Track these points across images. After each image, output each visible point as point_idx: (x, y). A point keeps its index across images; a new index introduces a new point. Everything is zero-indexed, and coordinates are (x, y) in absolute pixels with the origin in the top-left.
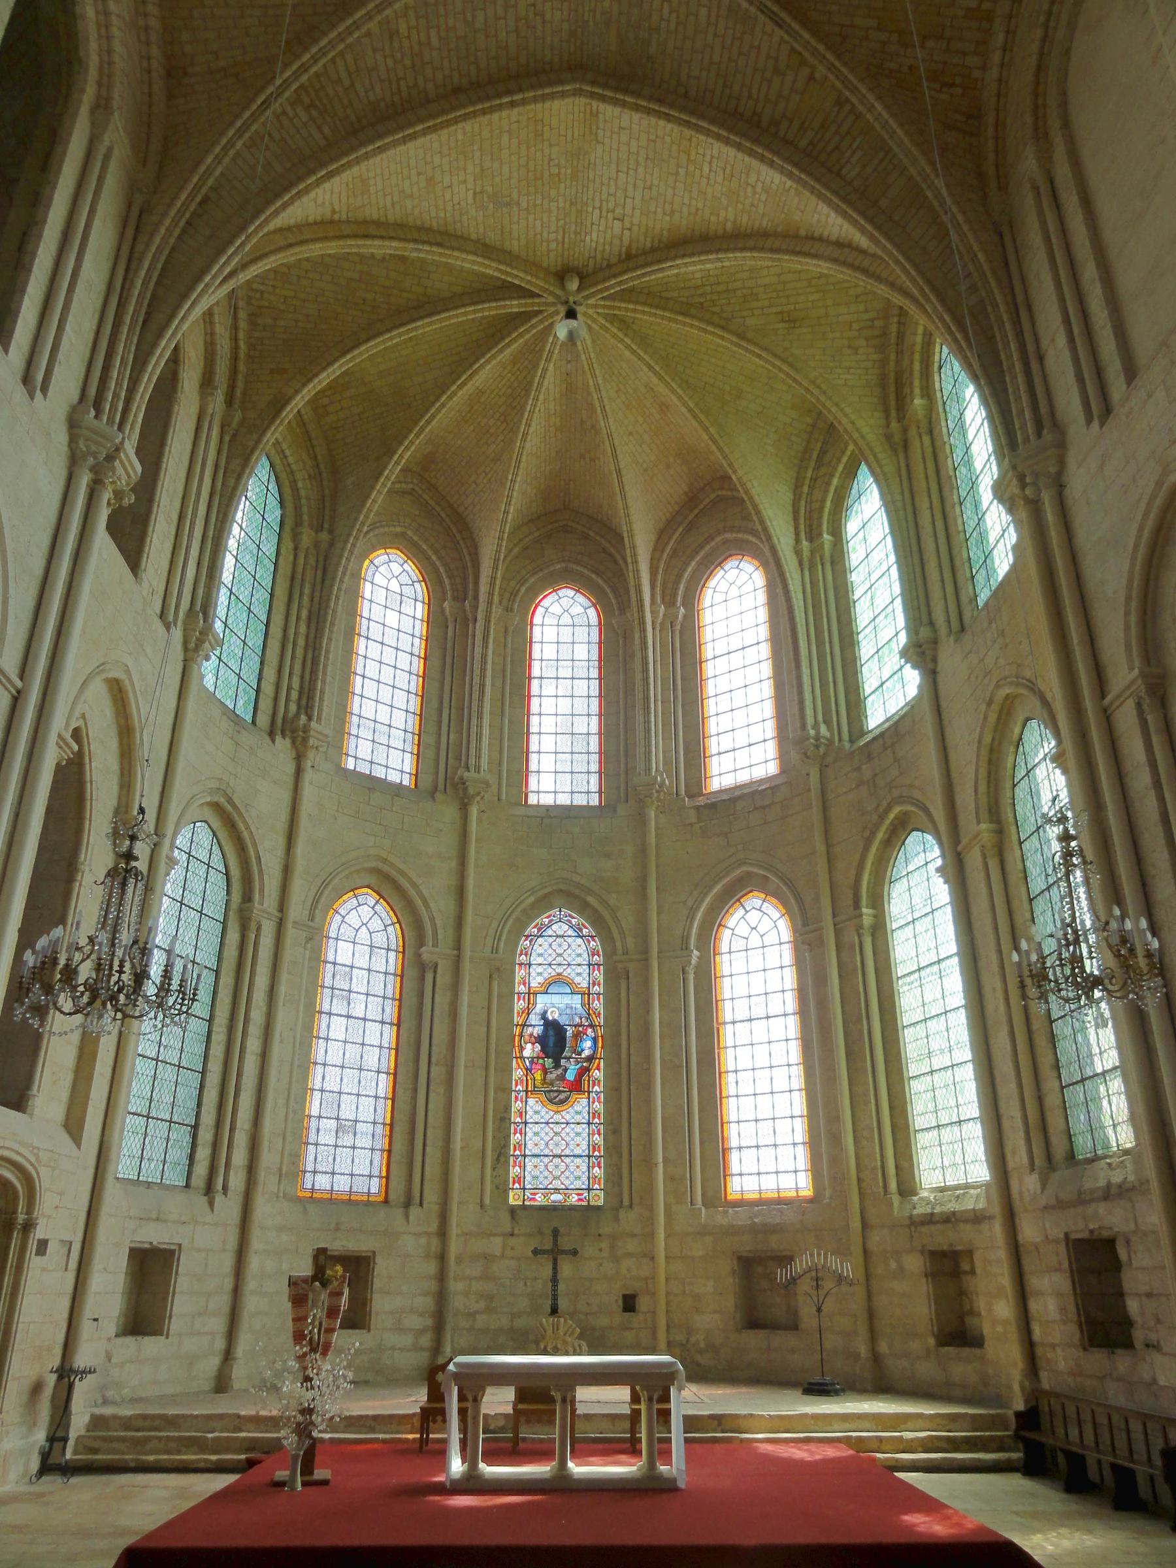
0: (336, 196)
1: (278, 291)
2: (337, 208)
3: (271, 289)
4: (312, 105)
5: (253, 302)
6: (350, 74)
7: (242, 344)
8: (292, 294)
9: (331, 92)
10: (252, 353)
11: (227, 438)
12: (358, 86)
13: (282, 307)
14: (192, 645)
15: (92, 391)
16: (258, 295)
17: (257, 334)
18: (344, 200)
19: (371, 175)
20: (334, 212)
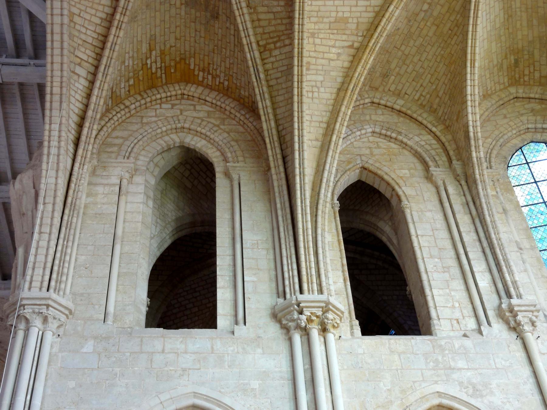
0: (338, 44)
1: (424, 84)
2: (350, 43)
3: (422, 89)
4: (274, 43)
5: (424, 103)
6: (269, 12)
7: (434, 129)
8: (429, 76)
9: (272, 28)
10: (447, 124)
11: (463, 183)
12: (275, 10)
13: (434, 87)
14: (512, 323)
15: (281, 289)
16: (422, 98)
17: (440, 114)
18: (344, 37)
19: (334, 14)
20: (351, 47)
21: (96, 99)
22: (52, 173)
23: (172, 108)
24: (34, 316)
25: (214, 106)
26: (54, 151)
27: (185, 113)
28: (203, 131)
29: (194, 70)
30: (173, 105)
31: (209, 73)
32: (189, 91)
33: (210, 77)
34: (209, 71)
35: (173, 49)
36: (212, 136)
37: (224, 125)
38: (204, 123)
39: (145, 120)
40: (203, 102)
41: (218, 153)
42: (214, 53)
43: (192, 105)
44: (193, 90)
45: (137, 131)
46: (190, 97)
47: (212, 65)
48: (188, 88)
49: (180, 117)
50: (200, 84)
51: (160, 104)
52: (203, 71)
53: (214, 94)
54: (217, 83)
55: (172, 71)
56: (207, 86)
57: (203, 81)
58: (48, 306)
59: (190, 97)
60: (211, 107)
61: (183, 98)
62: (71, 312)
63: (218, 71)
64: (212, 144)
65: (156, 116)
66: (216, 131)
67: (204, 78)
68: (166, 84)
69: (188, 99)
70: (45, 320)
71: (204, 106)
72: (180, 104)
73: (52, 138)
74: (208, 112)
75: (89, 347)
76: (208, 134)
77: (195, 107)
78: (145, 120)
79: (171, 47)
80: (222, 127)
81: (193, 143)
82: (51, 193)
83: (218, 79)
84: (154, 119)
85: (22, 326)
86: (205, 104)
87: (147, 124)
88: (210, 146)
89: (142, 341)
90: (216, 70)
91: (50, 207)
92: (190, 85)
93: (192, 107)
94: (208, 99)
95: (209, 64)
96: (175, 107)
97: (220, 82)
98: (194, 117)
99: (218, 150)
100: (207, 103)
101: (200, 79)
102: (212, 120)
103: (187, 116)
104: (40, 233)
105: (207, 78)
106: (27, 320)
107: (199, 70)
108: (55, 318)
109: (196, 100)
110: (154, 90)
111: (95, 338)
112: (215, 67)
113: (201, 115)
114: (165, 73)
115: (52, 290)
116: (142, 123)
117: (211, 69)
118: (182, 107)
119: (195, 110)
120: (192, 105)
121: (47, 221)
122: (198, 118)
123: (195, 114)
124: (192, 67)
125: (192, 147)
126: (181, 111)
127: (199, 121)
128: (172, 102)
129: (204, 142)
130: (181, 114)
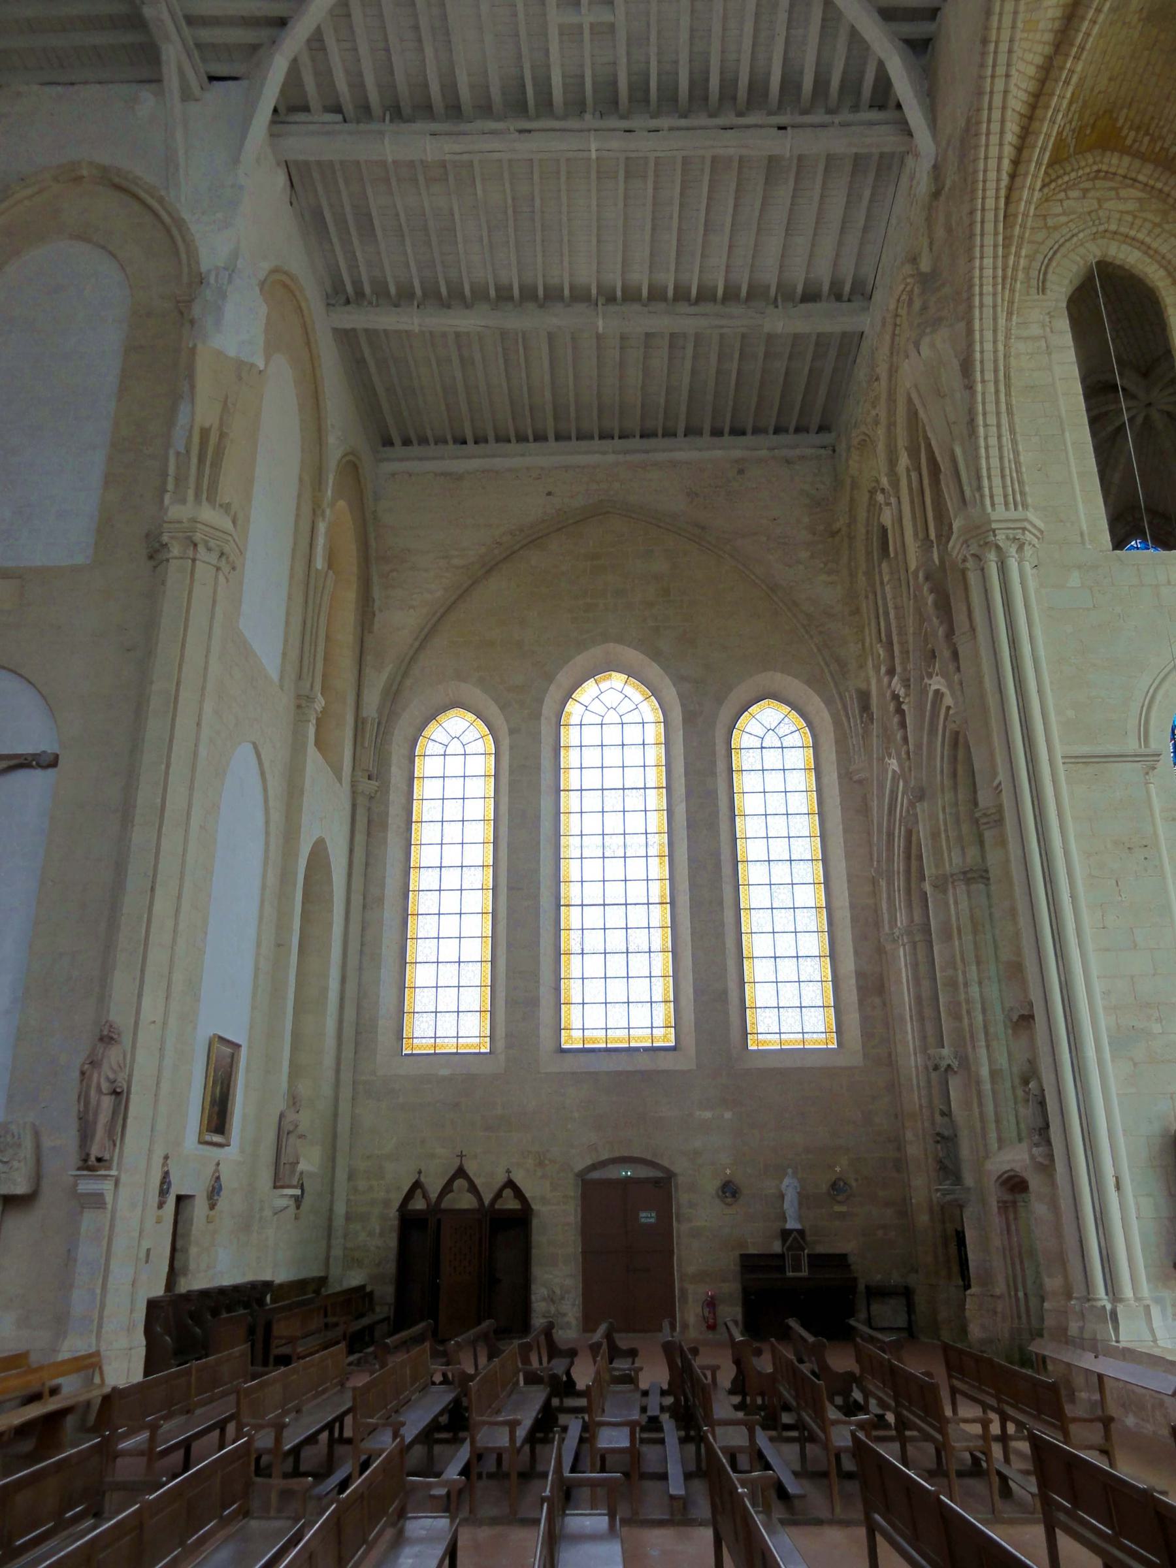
21: (1025, 206)
22: (989, 335)
23: (1084, 197)
24: (1009, 543)
25: (1149, 189)
26: (988, 300)
27: (1107, 205)
28: (1140, 236)
29: (1121, 128)
30: (1085, 191)
31: (1147, 133)
32: (1110, 165)
33: (1147, 139)
34: (1148, 129)
35: (1101, 96)
36: (1155, 245)
37: (1168, 222)
38: (1138, 222)
39: (1050, 222)
40: (1130, 182)
41: (1162, 273)
42: (1168, 99)
43: (1111, 189)
44: (1115, 162)
45: (1043, 243)
46: (1109, 175)
47: (1156, 121)
48: (1106, 160)
49: (1101, 213)
50: (1125, 151)
51: (1065, 191)
52: (1138, 129)
53: (1149, 168)
54: (1157, 149)
55: (1088, 132)
56: (1137, 155)
57: (1131, 147)
58: (1024, 529)
59: (1109, 175)
60: (1142, 191)
61: (1096, 178)
62: (1042, 532)
63: (1165, 130)
64: (1151, 257)
65: (1064, 213)
66: (1158, 235)
67: (1134, 141)
68: (1075, 153)
69: (1104, 178)
70: (1021, 548)
71: (1131, 190)
72: (1094, 188)
73: (985, 281)
74: (1140, 200)
75: (1074, 579)
76: (1148, 240)
77: (1118, 194)
78: (1050, 222)
79: (1099, 93)
80: (1167, 227)
81: (1121, 256)
82: (989, 366)
83: (1159, 144)
84: (1064, 219)
85: (992, 556)
86: (1132, 186)
87: (1055, 228)
88: (1148, 260)
89: (1138, 570)
90: (1163, 127)
91: (991, 388)
92: (1108, 154)
93: (1113, 193)
94: (1141, 178)
95: (1152, 118)
96: (1090, 195)
97: (1162, 148)
98: (1122, 212)
99: (1162, 266)
100: (1137, 185)
101: (1129, 142)
102: (1150, 216)
103: (1110, 211)
104: (986, 425)
105: (1141, 142)
106: (998, 548)
107: (1131, 128)
108: (1030, 544)
109: (1119, 178)
110: (1057, 167)
111: (1079, 567)
112: (1161, 123)
113: (1131, 206)
114: (1077, 138)
115: (1020, 508)
116: (1046, 226)
117: (1153, 125)
118: (1098, 194)
119: (1119, 198)
120: (1111, 189)
121: (991, 407)
122: (1128, 212)
123: (1121, 207)
124: (1120, 123)
125: (1118, 262)
126: (1099, 200)
127: (1129, 218)
128: (1082, 186)
129: (1137, 254)
130: (1100, 207)
